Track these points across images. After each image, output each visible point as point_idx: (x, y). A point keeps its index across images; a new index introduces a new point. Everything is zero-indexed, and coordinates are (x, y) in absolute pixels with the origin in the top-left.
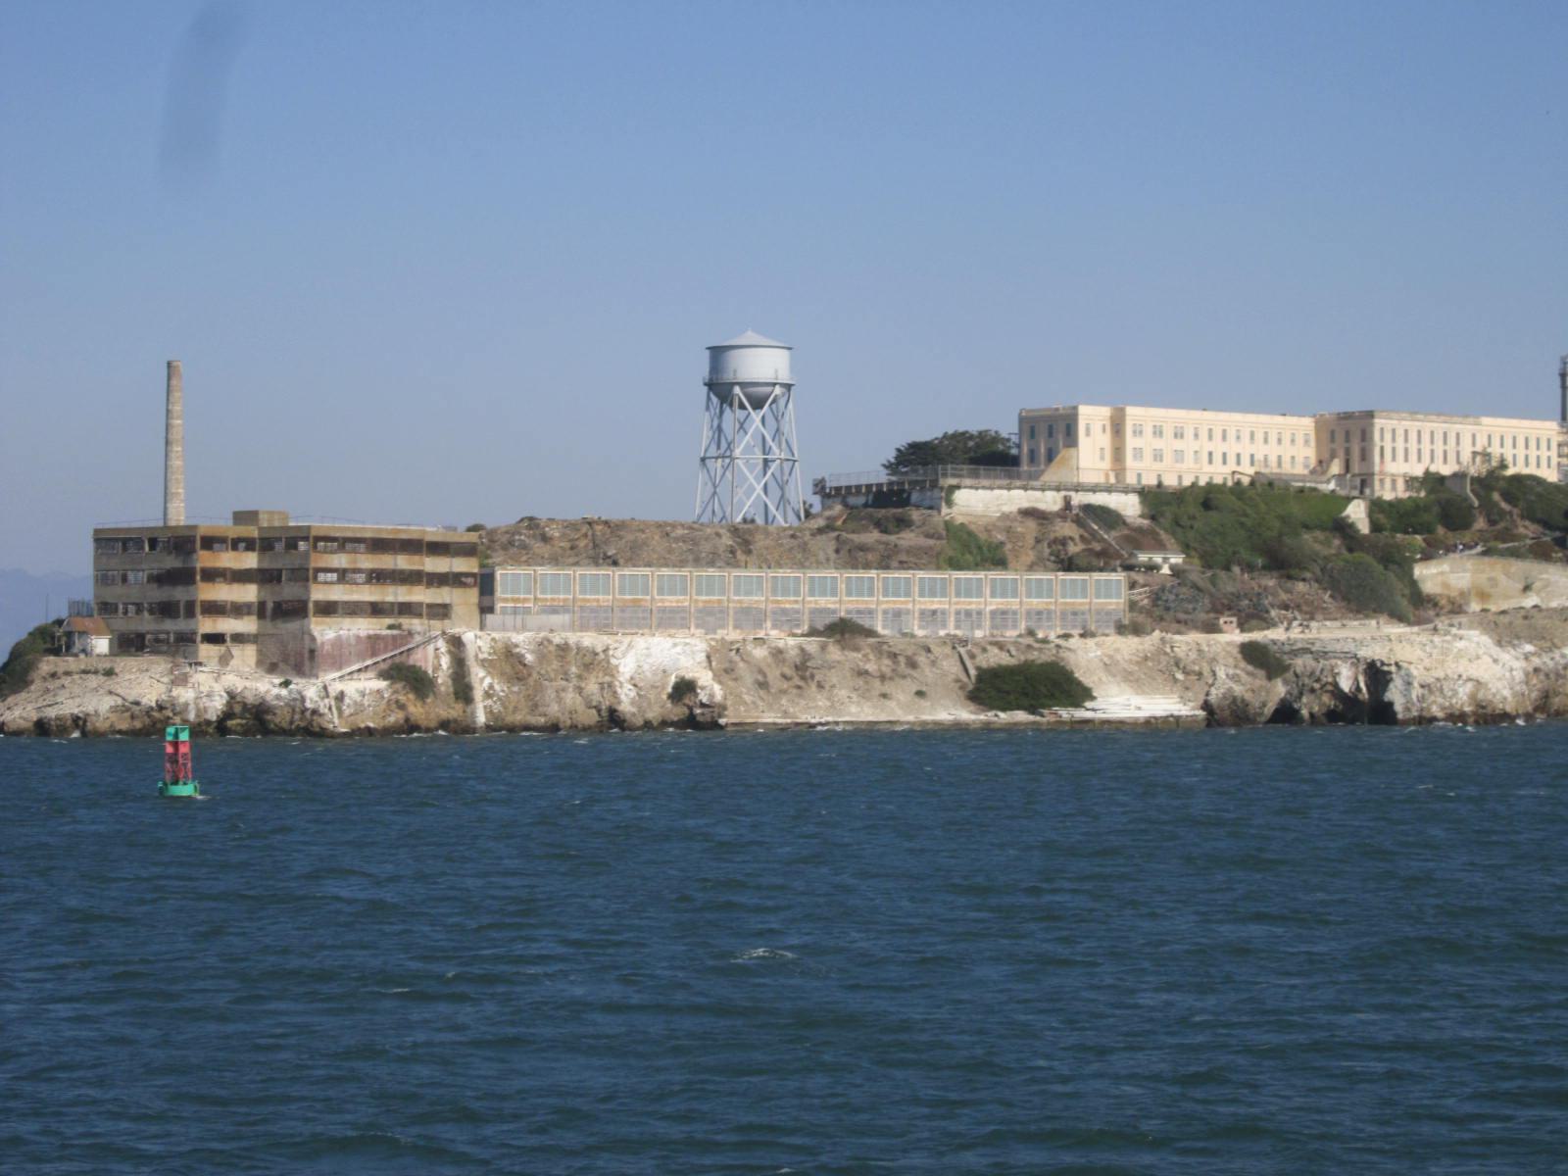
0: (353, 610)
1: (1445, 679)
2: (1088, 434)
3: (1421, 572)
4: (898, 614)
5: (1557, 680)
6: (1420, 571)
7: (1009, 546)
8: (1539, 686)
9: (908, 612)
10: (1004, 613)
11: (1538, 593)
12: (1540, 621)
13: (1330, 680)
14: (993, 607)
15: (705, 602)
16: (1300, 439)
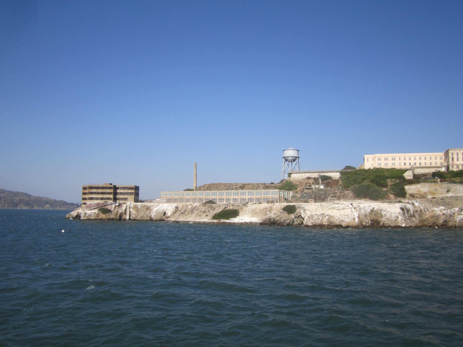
0: (97, 199)
1: (315, 215)
2: (368, 161)
3: (408, 188)
4: (228, 199)
5: (450, 217)
6: (406, 187)
7: (299, 185)
8: (444, 219)
9: (231, 199)
10: (251, 199)
11: (452, 192)
12: (447, 200)
13: (299, 214)
14: (248, 198)
15: (193, 197)
16: (438, 158)
